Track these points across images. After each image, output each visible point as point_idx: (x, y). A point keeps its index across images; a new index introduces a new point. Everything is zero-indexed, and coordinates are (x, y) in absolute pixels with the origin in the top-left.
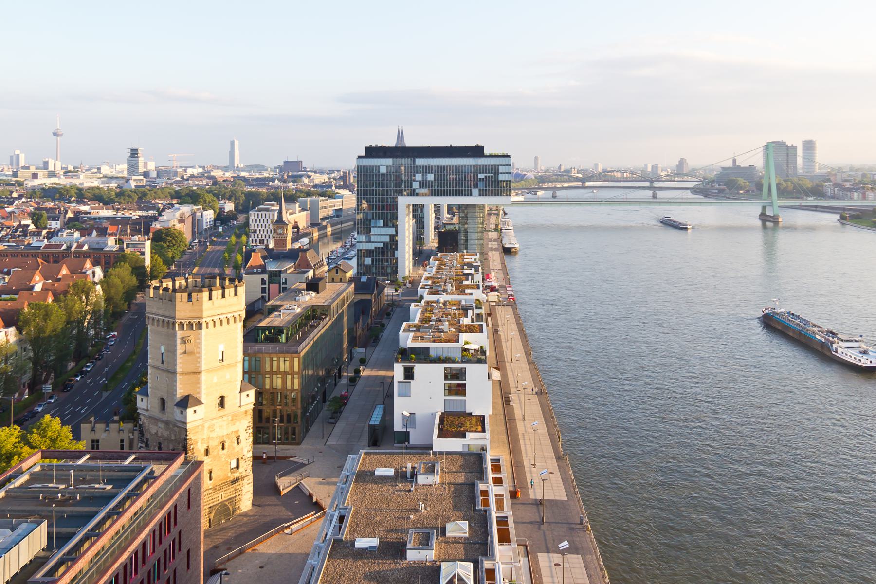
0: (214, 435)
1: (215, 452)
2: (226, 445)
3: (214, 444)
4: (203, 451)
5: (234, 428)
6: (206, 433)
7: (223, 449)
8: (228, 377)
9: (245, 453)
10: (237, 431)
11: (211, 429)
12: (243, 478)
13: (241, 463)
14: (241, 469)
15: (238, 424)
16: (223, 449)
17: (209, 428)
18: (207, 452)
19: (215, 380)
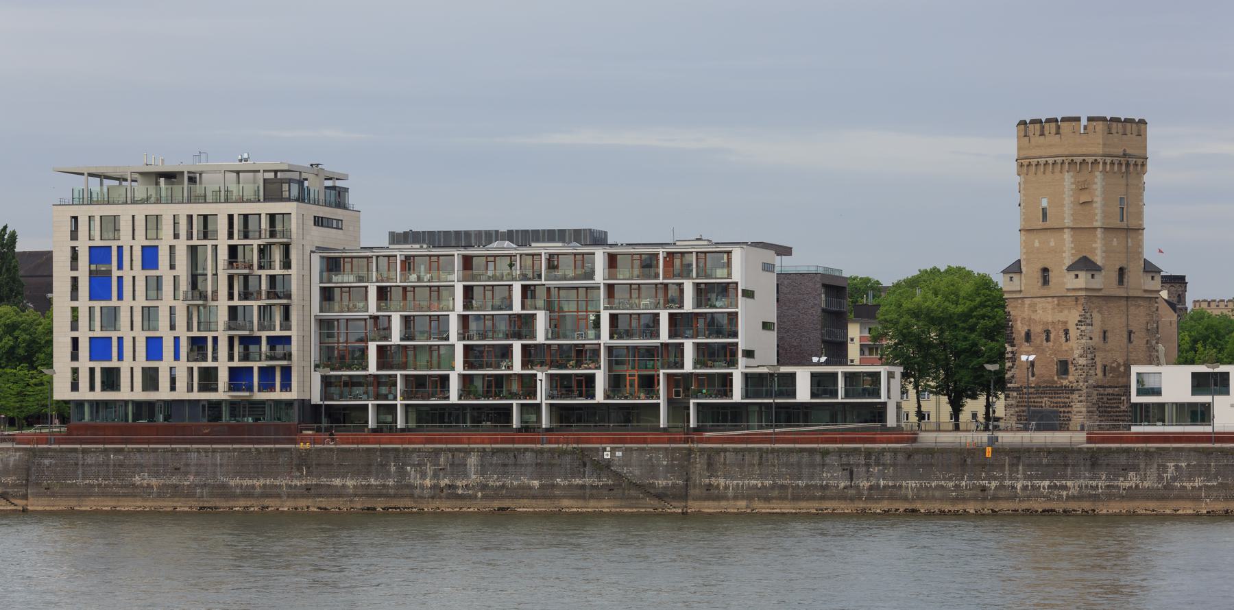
0: (1036, 317)
1: (1038, 341)
2: (1052, 336)
3: (1037, 329)
4: (1023, 334)
5: (1061, 317)
6: (1026, 312)
7: (1048, 340)
8: (1052, 244)
9: (1076, 356)
10: (1066, 323)
11: (1033, 308)
12: (1072, 391)
13: (1071, 369)
14: (1071, 378)
15: (1066, 312)
16: (1048, 340)
17: (1030, 306)
18: (1028, 336)
19: (1037, 244)
